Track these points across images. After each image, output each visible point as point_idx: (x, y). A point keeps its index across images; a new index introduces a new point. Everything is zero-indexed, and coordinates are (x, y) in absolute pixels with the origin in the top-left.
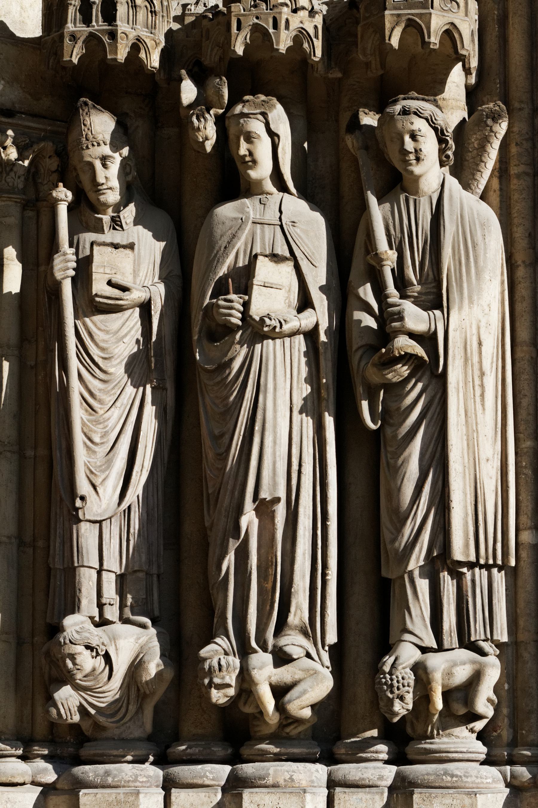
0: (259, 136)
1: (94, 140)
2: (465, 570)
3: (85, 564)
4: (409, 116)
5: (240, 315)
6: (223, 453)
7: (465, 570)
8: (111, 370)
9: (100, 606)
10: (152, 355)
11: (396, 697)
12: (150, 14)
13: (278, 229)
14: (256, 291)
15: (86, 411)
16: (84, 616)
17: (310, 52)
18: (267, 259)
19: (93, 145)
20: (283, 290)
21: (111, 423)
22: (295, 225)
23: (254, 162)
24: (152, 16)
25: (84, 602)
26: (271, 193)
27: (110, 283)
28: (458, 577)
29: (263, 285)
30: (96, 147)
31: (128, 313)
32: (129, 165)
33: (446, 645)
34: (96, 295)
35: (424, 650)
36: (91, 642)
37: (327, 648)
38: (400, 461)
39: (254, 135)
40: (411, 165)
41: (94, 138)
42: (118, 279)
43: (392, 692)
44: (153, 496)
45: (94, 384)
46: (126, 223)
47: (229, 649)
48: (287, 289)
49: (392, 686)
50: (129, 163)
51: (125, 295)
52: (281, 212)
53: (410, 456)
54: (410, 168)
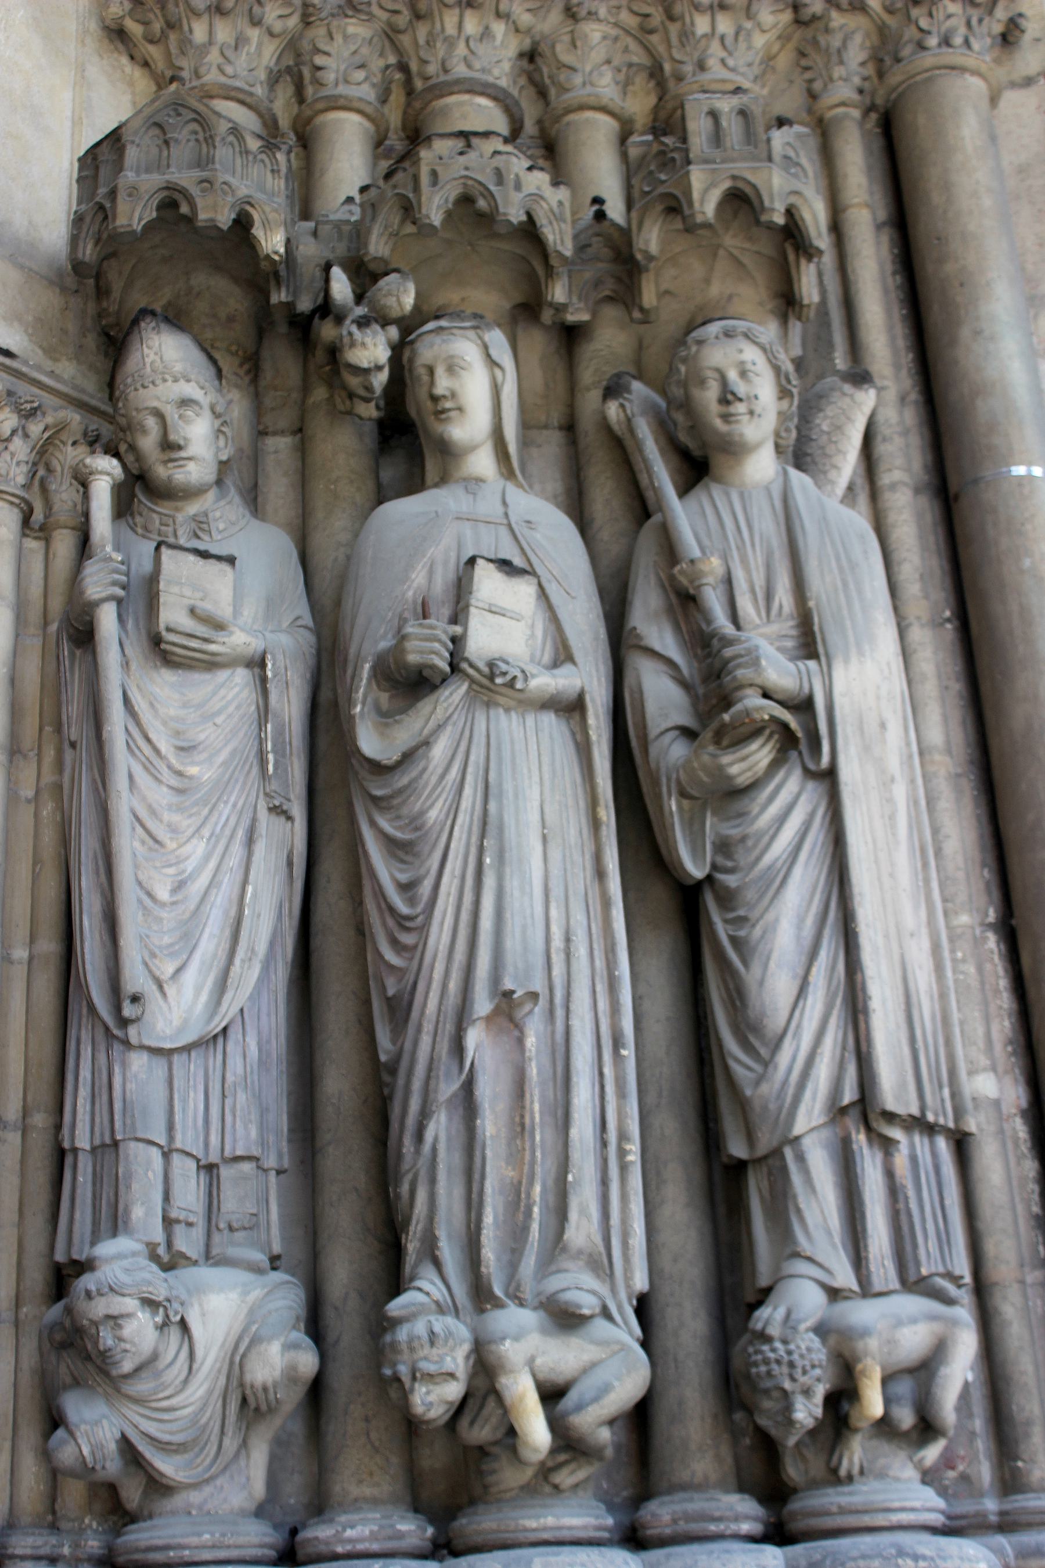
0: (470, 364)
2: (896, 1133)
3: (140, 1135)
5: (447, 655)
6: (416, 917)
7: (896, 1133)
8: (193, 770)
9: (168, 1222)
10: (269, 748)
11: (798, 1390)
13: (504, 531)
16: (137, 1240)
18: (491, 566)
20: (523, 623)
21: (190, 866)
23: (460, 409)
25: (138, 1213)
27: (193, 611)
28: (887, 1145)
29: (487, 607)
30: (169, 383)
31: (222, 675)
32: (224, 433)
33: (878, 1285)
34: (169, 630)
35: (834, 1294)
36: (156, 1292)
37: (635, 1302)
38: (757, 932)
39: (462, 364)
41: (165, 367)
42: (206, 606)
43: (793, 1379)
44: (269, 1015)
47: (445, 1301)
48: (530, 622)
49: (792, 1365)
50: (223, 429)
51: (220, 636)
52: (504, 503)
53: (777, 920)
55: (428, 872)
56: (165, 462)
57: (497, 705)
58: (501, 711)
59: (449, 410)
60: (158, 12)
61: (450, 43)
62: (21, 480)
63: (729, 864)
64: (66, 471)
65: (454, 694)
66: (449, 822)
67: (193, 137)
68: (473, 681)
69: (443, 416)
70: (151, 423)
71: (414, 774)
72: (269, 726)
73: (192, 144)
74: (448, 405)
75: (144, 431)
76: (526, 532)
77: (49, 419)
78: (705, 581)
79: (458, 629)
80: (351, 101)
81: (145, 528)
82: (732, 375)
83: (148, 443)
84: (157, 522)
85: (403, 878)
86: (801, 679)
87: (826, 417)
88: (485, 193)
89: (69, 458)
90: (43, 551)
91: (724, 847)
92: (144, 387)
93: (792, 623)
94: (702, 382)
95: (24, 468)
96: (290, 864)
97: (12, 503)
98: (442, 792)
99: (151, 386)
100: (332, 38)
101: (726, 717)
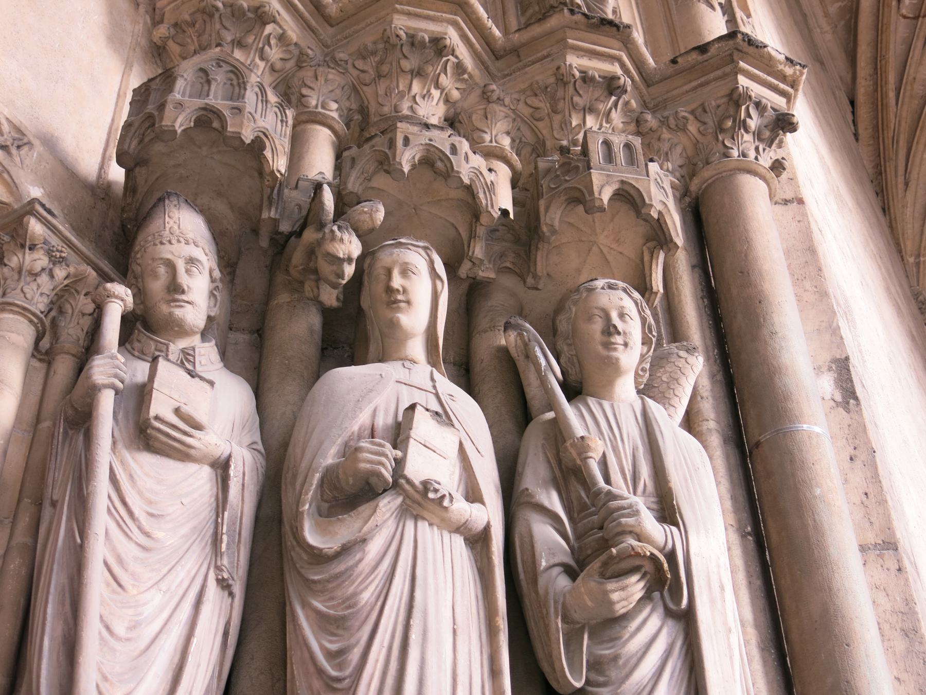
1: (181, 235)
4: (617, 292)
6: (344, 679)
8: (159, 534)
10: (224, 531)
12: (279, 123)
14: (413, 447)
15: (108, 585)
17: (487, 204)
19: (179, 241)
21: (148, 610)
22: (454, 399)
23: (408, 302)
24: (282, 126)
26: (416, 360)
27: (177, 411)
30: (183, 244)
31: (192, 467)
32: (215, 296)
34: (157, 418)
39: (414, 270)
40: (615, 349)
45: (128, 549)
46: (200, 363)
50: (215, 292)
54: (614, 354)
55: (358, 642)
56: (168, 302)
57: (424, 519)
58: (427, 523)
59: (400, 301)
60: (195, 39)
61: (402, 95)
62: (42, 307)
63: (601, 679)
64: (75, 314)
65: (388, 505)
66: (379, 604)
67: (229, 82)
68: (407, 496)
69: (395, 306)
70: (162, 270)
71: (351, 563)
72: (226, 514)
73: (228, 86)
74: (400, 297)
75: (156, 276)
76: (450, 402)
77: (72, 270)
78: (590, 454)
79: (399, 454)
80: (326, 118)
81: (142, 352)
82: (614, 316)
83: (157, 286)
84: (153, 347)
85: (333, 647)
86: (666, 536)
87: (665, 372)
88: (443, 158)
89: (80, 304)
90: (44, 371)
91: (596, 665)
92: (162, 243)
93: (653, 499)
94: (590, 318)
95: (46, 300)
96: (226, 634)
97: (31, 321)
98: (375, 578)
99: (167, 243)
100: (317, 79)
101: (614, 551)
